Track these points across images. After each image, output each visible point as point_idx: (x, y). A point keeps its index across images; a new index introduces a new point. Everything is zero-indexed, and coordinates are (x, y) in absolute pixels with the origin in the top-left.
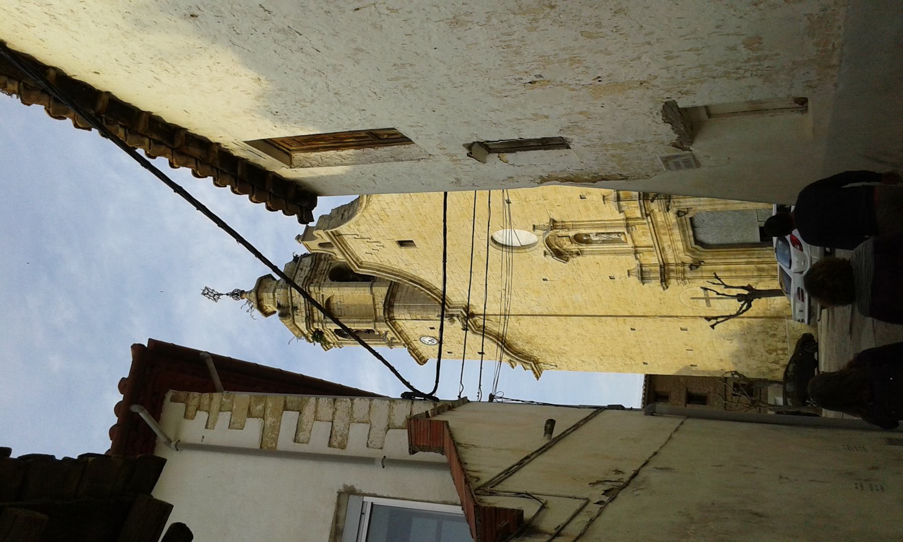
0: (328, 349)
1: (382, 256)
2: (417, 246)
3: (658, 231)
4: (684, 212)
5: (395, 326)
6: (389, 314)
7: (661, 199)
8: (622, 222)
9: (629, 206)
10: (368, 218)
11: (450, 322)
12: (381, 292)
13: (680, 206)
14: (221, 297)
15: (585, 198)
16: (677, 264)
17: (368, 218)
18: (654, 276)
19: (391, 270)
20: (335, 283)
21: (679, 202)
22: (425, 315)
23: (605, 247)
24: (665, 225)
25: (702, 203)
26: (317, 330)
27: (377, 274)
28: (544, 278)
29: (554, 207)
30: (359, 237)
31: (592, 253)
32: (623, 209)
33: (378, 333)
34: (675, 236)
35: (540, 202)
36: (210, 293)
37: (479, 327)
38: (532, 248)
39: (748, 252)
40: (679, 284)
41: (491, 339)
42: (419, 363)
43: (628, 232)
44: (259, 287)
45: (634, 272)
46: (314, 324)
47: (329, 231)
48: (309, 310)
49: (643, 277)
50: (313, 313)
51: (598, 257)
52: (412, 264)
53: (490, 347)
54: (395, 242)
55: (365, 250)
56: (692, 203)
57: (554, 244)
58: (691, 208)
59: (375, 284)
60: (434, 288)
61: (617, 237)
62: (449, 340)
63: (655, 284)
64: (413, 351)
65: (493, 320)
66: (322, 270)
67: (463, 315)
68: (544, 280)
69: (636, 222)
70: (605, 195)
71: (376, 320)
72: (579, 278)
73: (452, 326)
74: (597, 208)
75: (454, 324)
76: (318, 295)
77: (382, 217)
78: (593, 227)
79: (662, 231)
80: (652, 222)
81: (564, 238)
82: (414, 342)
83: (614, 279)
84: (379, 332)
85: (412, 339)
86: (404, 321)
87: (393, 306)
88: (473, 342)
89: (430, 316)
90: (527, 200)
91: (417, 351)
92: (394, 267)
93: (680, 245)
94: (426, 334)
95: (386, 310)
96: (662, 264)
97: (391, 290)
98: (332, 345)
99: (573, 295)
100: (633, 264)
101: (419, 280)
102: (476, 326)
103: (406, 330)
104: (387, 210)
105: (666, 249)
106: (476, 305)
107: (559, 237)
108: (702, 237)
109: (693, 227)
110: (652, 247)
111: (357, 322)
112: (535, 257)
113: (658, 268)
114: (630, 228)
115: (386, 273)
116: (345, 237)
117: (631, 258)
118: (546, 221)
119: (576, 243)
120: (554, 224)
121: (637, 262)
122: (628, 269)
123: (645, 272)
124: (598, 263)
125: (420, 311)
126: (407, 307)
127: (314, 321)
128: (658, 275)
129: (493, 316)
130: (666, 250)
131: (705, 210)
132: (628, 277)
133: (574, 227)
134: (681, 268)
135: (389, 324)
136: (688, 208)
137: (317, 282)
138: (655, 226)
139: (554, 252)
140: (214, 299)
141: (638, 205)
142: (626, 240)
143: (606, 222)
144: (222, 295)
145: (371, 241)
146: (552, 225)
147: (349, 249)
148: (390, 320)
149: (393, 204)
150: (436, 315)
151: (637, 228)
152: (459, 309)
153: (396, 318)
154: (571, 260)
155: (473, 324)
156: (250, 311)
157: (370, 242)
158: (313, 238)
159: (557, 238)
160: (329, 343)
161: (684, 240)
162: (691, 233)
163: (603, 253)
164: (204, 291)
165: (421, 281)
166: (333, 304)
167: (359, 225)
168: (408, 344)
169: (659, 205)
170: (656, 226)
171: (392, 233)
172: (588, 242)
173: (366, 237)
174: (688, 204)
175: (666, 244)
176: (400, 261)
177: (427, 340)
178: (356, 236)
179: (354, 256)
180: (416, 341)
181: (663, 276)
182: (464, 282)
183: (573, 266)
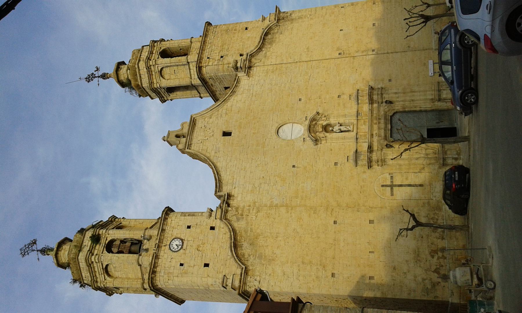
90: (310, 99)
105: (374, 135)
130: (374, 137)
147: (192, 135)
162: (390, 127)
179: (191, 142)
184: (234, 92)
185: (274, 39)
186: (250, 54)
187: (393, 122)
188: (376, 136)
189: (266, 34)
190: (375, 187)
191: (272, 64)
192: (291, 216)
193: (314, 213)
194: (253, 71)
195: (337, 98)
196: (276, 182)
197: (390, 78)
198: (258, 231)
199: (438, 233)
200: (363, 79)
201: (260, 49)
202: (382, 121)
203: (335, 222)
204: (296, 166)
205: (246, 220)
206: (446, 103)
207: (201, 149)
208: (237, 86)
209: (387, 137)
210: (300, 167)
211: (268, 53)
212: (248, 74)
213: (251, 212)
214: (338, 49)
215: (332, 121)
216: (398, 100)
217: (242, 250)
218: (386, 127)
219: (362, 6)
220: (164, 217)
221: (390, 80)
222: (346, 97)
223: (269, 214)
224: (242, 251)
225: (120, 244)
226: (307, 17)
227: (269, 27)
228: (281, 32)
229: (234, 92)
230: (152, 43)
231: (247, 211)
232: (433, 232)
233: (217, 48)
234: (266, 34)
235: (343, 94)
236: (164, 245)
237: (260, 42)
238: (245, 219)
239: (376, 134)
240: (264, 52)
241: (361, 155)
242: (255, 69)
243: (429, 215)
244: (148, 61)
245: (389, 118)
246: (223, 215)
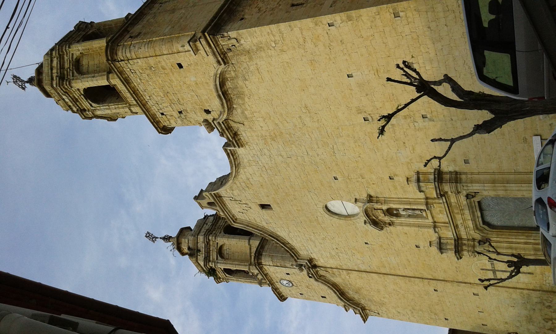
0: (219, 283)
1: (250, 215)
2: (274, 209)
3: (452, 210)
4: (473, 195)
5: (262, 269)
6: (258, 260)
7: (452, 183)
8: (423, 200)
9: (427, 187)
10: (239, 185)
11: (299, 270)
12: (255, 243)
13: (468, 190)
14: (157, 239)
15: (393, 179)
16: (468, 239)
17: (239, 185)
18: (450, 247)
19: (256, 226)
20: (227, 235)
21: (467, 186)
22: (282, 263)
23: (411, 220)
24: (458, 206)
25: (486, 188)
26: (211, 267)
27: (246, 228)
28: (366, 242)
29: (370, 185)
30: (234, 199)
31: (401, 224)
32: (423, 189)
33: (251, 274)
34: (466, 216)
35: (360, 180)
36: (150, 236)
37: (320, 276)
38: (356, 217)
39: (526, 234)
40: (470, 256)
41: (329, 287)
42: (279, 299)
43: (428, 210)
44: (180, 234)
45: (434, 243)
46: (210, 263)
47: (212, 193)
48: (207, 253)
49: (441, 248)
50: (210, 255)
51: (406, 229)
52: (270, 223)
53: (329, 293)
54: (258, 205)
55: (238, 210)
56: (478, 188)
57: (371, 215)
58: (478, 192)
59: (252, 238)
60: (287, 243)
61: (420, 213)
62: (300, 284)
63: (450, 255)
64: (275, 290)
65: (330, 272)
66: (219, 226)
67: (308, 265)
68: (366, 243)
69: (434, 201)
70: (409, 177)
71: (250, 264)
72: (392, 244)
73: (301, 274)
74: (402, 188)
75: (303, 273)
76: (214, 242)
77: (248, 185)
78: (401, 203)
79: (456, 211)
80: (447, 202)
81: (379, 210)
82: (276, 283)
83: (419, 247)
84: (252, 273)
85: (275, 281)
86: (268, 267)
87: (261, 255)
88: (317, 288)
89: (286, 264)
90: (350, 178)
91: (278, 290)
92: (258, 224)
93: (470, 224)
94: (284, 278)
95: (256, 257)
96: (456, 238)
97: (261, 243)
98: (222, 280)
99: (388, 257)
100: (434, 237)
101: (276, 236)
102: (318, 275)
103: (270, 274)
104: (251, 180)
105: (460, 226)
106: (318, 259)
107: (375, 209)
108: (488, 219)
109: (481, 210)
110: (448, 223)
111: (238, 265)
112: (358, 224)
113: (453, 242)
114: (429, 206)
115: (253, 228)
116: (224, 199)
117: (431, 230)
118: (364, 196)
119: (388, 216)
120: (370, 199)
121: (436, 234)
122: (430, 240)
123: (443, 244)
124: (406, 234)
125: (279, 260)
126: (271, 256)
127: (210, 261)
128: (453, 247)
129: (330, 269)
130: (459, 227)
131: (490, 196)
132: (429, 246)
133: (385, 202)
134: (472, 243)
135: (258, 268)
136: (475, 193)
137: (214, 234)
138: (449, 205)
139: (371, 221)
140: (153, 241)
141: (434, 187)
142: (427, 216)
143: (410, 200)
144: (158, 238)
145: (242, 203)
146: (369, 199)
147: (227, 208)
148: (259, 265)
149: (255, 175)
150: (290, 264)
151: (435, 207)
152: (305, 261)
153: (263, 263)
154: (385, 229)
155: (316, 273)
156: (172, 251)
157: (241, 204)
158: (204, 198)
159: (374, 210)
160: (220, 278)
161: (474, 220)
162: (479, 214)
163: (409, 225)
164: (146, 234)
165: (277, 237)
166: (224, 250)
167: (233, 190)
168: (271, 284)
169: (451, 188)
170: (450, 206)
171: (256, 197)
172: (398, 215)
173: (238, 200)
174: (475, 188)
175: (459, 222)
176: (262, 220)
177: (285, 282)
178: (231, 199)
179: (231, 214)
180: (277, 282)
181: (456, 248)
182: (308, 240)
183: (387, 234)
184: (238, 164)
188: (462, 226)
189: (222, 84)
202: (467, 212)
208: (236, 158)
212: (240, 145)
218: (474, 215)
219: (372, 22)
220: (259, 268)
226: (272, 49)
227: (218, 76)
229: (238, 164)
230: (62, 90)
234: (222, 84)
237: (222, 105)
239: (461, 224)
240: (239, 111)
244: (84, 114)
246: (316, 277)
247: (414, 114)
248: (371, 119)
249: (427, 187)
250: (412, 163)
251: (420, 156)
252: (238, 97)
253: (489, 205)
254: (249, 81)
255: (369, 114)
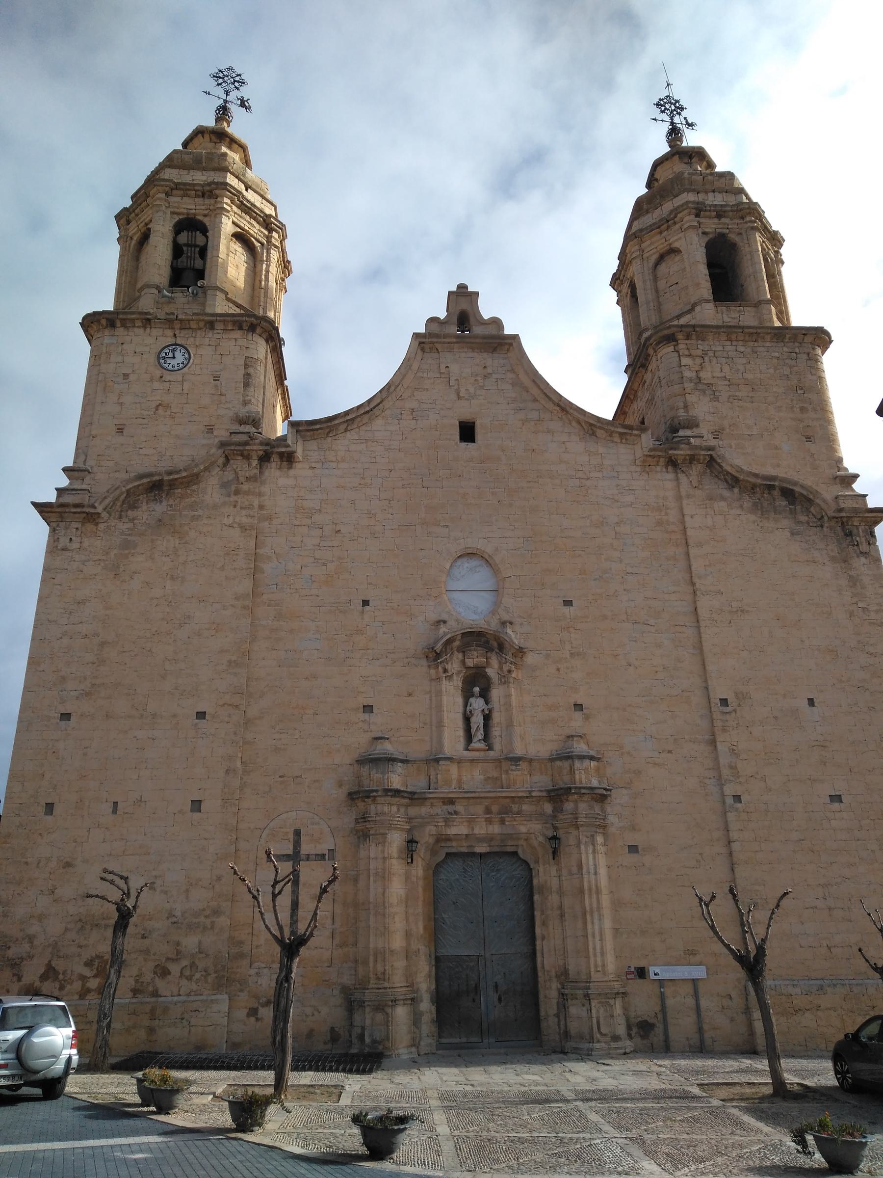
90: (571, 630)
124: (410, 695)
130: (446, 807)
185: (772, 515)
186: (714, 456)
187: (501, 860)
190: (294, 813)
191: (687, 519)
192: (225, 608)
193: (230, 662)
194: (661, 471)
195: (572, 701)
196: (325, 564)
197: (640, 848)
198: (192, 534)
199: (153, 979)
200: (638, 773)
201: (733, 481)
203: (201, 715)
204: (367, 608)
205: (224, 504)
206: (554, 1015)
207: (425, 375)
209: (449, 844)
210: (363, 619)
211: (723, 504)
213: (244, 512)
214: (741, 697)
215: (496, 693)
216: (564, 872)
217: (147, 503)
221: (633, 849)
222: (577, 723)
223: (237, 555)
224: (144, 504)
225: (196, 246)
226: (855, 600)
228: (798, 534)
231: (247, 503)
232: (156, 966)
233: (738, 370)
235: (587, 718)
236: (177, 332)
238: (227, 499)
240: (726, 493)
241: (382, 773)
242: (671, 476)
243: (203, 955)
245: (509, 849)
247: (740, 783)
248: (725, 711)
249: (583, 772)
250: (622, 754)
251: (640, 772)
252: (755, 505)
253: (498, 871)
254: (790, 538)
255: (735, 711)
